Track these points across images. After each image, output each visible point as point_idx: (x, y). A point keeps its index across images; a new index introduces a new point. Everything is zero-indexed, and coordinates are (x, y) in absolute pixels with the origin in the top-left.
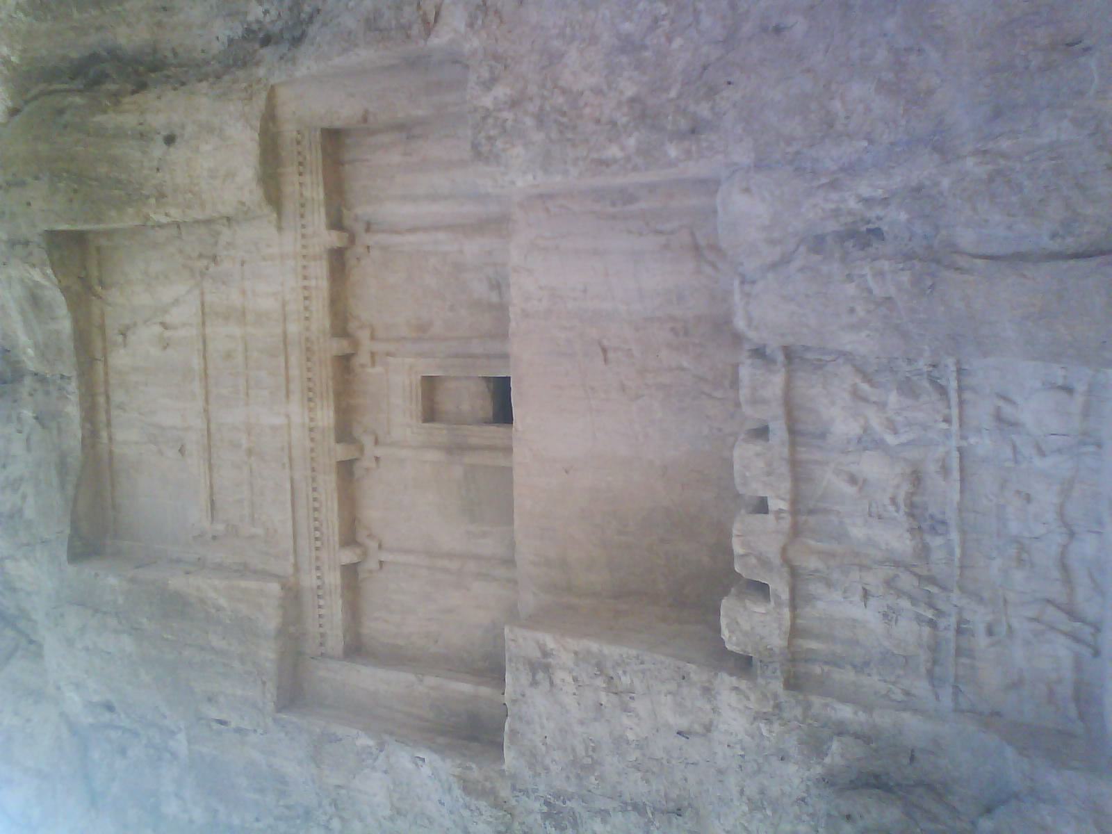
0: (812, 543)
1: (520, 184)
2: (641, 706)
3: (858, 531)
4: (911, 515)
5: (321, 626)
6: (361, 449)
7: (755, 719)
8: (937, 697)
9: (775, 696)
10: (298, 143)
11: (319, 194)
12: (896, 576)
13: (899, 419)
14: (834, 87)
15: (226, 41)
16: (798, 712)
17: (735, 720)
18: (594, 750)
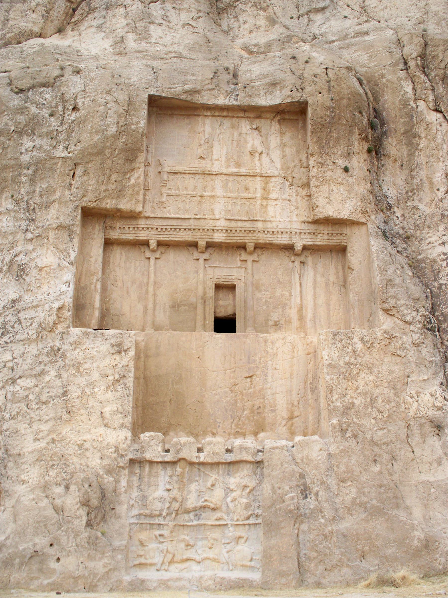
0: (187, 469)
1: (324, 353)
2: (109, 395)
3: (193, 487)
4: (201, 507)
5: (120, 228)
6: (202, 252)
7: (115, 446)
8: (132, 517)
9: (126, 455)
10: (341, 234)
11: (319, 242)
14: (355, 482)
15: (387, 194)
16: (121, 464)
18: (86, 372)
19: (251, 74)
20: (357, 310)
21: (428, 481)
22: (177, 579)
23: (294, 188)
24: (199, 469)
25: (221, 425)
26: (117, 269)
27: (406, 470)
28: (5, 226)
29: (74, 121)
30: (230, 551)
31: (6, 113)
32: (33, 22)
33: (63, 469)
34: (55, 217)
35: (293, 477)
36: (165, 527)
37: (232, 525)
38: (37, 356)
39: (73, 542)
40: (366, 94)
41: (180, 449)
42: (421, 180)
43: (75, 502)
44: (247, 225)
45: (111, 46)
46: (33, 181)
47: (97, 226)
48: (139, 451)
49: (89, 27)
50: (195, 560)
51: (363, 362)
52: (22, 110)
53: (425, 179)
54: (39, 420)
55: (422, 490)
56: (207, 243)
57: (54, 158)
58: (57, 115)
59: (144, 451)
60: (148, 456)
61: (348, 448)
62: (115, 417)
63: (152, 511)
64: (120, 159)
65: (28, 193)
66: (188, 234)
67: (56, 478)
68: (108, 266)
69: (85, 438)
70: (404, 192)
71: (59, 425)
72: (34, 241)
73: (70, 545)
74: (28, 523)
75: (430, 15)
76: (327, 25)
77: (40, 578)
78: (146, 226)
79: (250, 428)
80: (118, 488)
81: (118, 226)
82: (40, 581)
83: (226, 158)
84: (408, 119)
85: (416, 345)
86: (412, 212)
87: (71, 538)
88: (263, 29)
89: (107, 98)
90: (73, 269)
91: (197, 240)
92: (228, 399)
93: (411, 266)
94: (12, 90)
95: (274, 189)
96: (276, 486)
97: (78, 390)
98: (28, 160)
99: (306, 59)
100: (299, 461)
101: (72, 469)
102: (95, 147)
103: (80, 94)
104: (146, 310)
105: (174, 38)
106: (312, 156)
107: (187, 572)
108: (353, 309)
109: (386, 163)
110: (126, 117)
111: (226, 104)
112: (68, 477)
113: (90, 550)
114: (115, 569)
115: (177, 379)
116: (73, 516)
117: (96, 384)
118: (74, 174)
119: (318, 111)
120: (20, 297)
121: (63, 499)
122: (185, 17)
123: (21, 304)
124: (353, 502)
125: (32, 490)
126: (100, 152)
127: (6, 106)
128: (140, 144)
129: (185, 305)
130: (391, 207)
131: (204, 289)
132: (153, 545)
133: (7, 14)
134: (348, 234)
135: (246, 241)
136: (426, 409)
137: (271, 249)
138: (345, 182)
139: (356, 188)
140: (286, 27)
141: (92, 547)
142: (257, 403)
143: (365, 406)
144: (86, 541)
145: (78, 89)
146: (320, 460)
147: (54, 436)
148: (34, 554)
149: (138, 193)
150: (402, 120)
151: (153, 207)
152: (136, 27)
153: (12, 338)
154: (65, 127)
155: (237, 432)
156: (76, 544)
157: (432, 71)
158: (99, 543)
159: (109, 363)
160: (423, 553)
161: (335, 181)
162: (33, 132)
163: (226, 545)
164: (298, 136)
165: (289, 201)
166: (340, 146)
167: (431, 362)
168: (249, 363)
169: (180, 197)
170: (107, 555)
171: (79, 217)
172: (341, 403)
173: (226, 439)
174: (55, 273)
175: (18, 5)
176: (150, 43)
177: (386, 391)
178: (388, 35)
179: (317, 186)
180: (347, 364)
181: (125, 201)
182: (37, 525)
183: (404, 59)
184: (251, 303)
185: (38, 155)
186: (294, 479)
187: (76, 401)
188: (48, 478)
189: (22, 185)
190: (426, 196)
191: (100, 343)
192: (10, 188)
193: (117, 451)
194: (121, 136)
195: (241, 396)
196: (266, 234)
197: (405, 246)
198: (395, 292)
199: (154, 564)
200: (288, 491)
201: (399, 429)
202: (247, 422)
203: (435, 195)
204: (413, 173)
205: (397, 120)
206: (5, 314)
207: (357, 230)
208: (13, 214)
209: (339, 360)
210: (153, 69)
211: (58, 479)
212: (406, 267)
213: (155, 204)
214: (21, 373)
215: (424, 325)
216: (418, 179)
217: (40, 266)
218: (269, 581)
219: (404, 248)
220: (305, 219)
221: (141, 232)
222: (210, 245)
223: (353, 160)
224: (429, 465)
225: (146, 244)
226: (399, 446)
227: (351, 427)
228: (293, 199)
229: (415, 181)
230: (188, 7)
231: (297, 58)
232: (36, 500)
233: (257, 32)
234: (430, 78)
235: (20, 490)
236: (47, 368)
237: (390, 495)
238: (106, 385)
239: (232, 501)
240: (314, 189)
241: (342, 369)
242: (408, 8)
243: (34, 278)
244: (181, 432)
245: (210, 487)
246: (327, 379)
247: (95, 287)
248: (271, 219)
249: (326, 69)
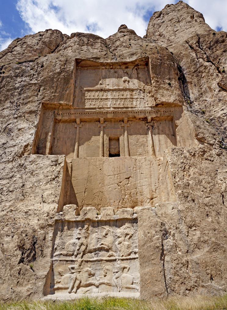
2: (48, 186)
3: (94, 236)
5: (62, 114)
9: (53, 218)
10: (170, 111)
12: (84, 245)
13: (122, 244)
16: (50, 223)
17: (47, 208)
25: (113, 204)
36: (75, 262)
37: (119, 260)
38: (12, 169)
41: (86, 213)
59: (65, 215)
61: (190, 207)
69: (30, 208)
70: (198, 95)
71: (17, 202)
73: (6, 275)
87: (7, 270)
96: (147, 231)
107: (90, 293)
117: (41, 180)
123: (7, 145)
133: (24, 51)
138: (169, 89)
139: (175, 91)
146: (173, 214)
158: (27, 274)
165: (143, 99)
170: (31, 282)
171: (40, 107)
180: (183, 163)
186: (158, 226)
187: (28, 189)
194: (62, 73)
195: (124, 188)
199: (67, 288)
200: (155, 234)
202: (127, 201)
204: (201, 87)
208: (9, 108)
211: (8, 232)
229: (203, 90)
236: (15, 174)
239: (119, 244)
245: (105, 235)
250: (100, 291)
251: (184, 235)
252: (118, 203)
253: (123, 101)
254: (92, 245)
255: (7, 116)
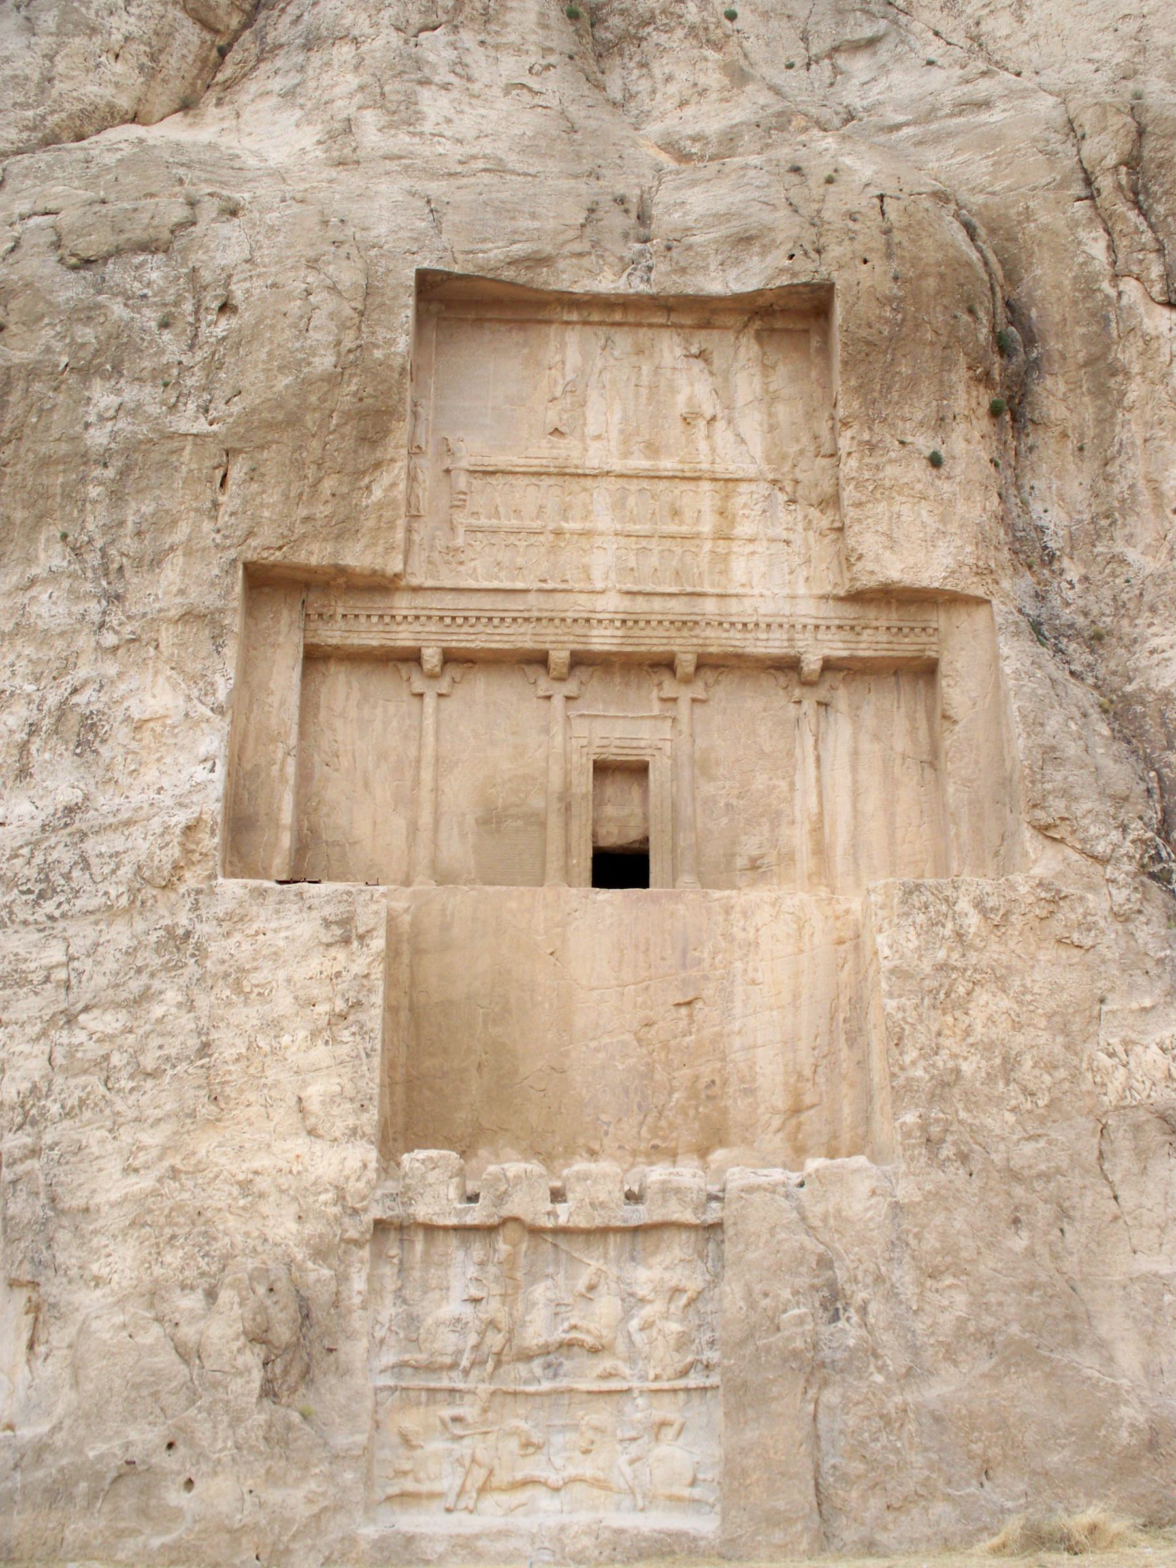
0: (524, 1246)
1: (881, 939)
2: (320, 1053)
3: (540, 1292)
4: (561, 1345)
5: (344, 616)
6: (561, 679)
7: (337, 1187)
8: (382, 1371)
10: (924, 629)
11: (864, 652)
13: (654, 1333)
14: (964, 1278)
16: (352, 1234)
18: (259, 994)
19: (685, 214)
20: (965, 828)
21: (1155, 1275)
22: (499, 1532)
23: (799, 510)
24: (555, 1246)
25: (612, 1130)
26: (338, 723)
27: (1099, 1245)
28: (46, 615)
29: (224, 338)
30: (639, 1459)
31: (46, 320)
32: (117, 84)
33: (201, 1247)
34: (175, 589)
35: (801, 1264)
38: (131, 953)
39: (227, 1438)
40: (986, 264)
41: (505, 1192)
42: (1131, 487)
43: (231, 1332)
44: (677, 607)
45: (319, 142)
46: (117, 497)
47: (285, 613)
48: (399, 1200)
49: (262, 95)
50: (545, 1484)
51: (984, 963)
52: (87, 313)
53: (1141, 484)
54: (137, 1120)
55: (1140, 1299)
56: (573, 654)
57: (171, 436)
58: (180, 325)
59: (410, 1199)
60: (422, 1211)
61: (944, 1187)
62: (335, 1111)
63: (432, 1355)
64: (343, 437)
65: (106, 528)
66: (522, 630)
67: (182, 1270)
68: (316, 716)
69: (256, 1165)
70: (1086, 517)
71: (188, 1132)
72: (120, 652)
73: (220, 1445)
74: (111, 1389)
75: (1152, 55)
76: (883, 83)
77: (140, 1532)
78: (413, 612)
79: (686, 1136)
80: (344, 1295)
81: (341, 611)
82: (141, 1539)
83: (622, 432)
84: (1094, 328)
85: (1120, 917)
86: (1107, 571)
87: (221, 1427)
88: (714, 96)
89: (309, 280)
90: (222, 724)
91: (547, 646)
92: (631, 1061)
93: (1106, 711)
94: (61, 260)
95: (747, 512)
97: (238, 1041)
98: (105, 442)
99: (828, 172)
100: (817, 1223)
101: (224, 1246)
102: (280, 406)
103: (239, 268)
104: (413, 828)
105: (484, 122)
106: (845, 424)
107: (527, 1515)
108: (956, 824)
109: (1040, 443)
110: (359, 328)
111: (621, 291)
112: (214, 1268)
113: (272, 1457)
114: (338, 1508)
115: (497, 1009)
116: (227, 1368)
117: (285, 1023)
118: (225, 476)
119: (861, 306)
120: (86, 798)
121: (202, 1324)
122: (510, 67)
124: (958, 1329)
125: (121, 1303)
126: (293, 421)
127: (47, 302)
128: (396, 397)
129: (516, 817)
130: (1052, 557)
131: (567, 774)
132: (437, 1445)
133: (48, 64)
134: (942, 629)
135: (675, 648)
136: (1148, 1084)
137: (739, 668)
138: (931, 493)
139: (961, 508)
140: (776, 90)
141: (277, 1450)
142: (706, 1071)
143: (990, 1078)
144: (261, 1433)
145: (233, 256)
146: (871, 1219)
147: (177, 1161)
148: (127, 1468)
149: (391, 526)
150: (1081, 330)
151: (430, 562)
152: (383, 94)
153: (65, 907)
154: (200, 355)
155: (655, 1147)
156: (236, 1442)
157: (1158, 201)
158: (296, 1440)
159: (319, 968)
160: (1144, 1463)
161: (906, 491)
162: (117, 370)
163: (626, 1444)
164: (808, 376)
165: (787, 542)
166: (919, 399)
167: (1160, 962)
168: (684, 966)
169: (502, 535)
170: (317, 1470)
171: (238, 589)
172: (926, 1070)
173: (626, 1166)
174: (176, 736)
175: (77, 40)
176: (422, 134)
177: (1044, 1037)
178: (1042, 108)
179: (859, 505)
180: (942, 967)
181: (359, 547)
182: (133, 1394)
183: (1085, 171)
184: (689, 811)
185: (130, 428)
186: (804, 1269)
187: (232, 1068)
188: (162, 1271)
189: (89, 507)
190: (1145, 527)
191: (295, 918)
192: (58, 514)
193: (341, 1198)
194: (346, 377)
195: (663, 1055)
196: (727, 631)
197: (1091, 658)
198: (1066, 778)
200: (789, 1301)
201: (1079, 1137)
202: (679, 1120)
203: (1168, 526)
204: (1110, 469)
205: (1068, 329)
206: (46, 844)
207: (964, 617)
208: (66, 584)
209: (920, 956)
210: (429, 202)
211: (187, 1273)
212: (1095, 714)
213: (436, 555)
214: (89, 996)
215: (1143, 866)
216: (1125, 484)
217: (136, 717)
218: (741, 1536)
219: (1089, 665)
220: (828, 589)
221: (401, 628)
222: (580, 661)
223: (954, 436)
224: (1158, 1231)
225: (413, 657)
226: (1078, 1182)
227: (952, 1133)
228: (797, 538)
229: (1116, 489)
230: (519, 41)
231: (805, 171)
232: (131, 1329)
233: (698, 103)
234: (1153, 220)
235: (87, 1302)
236: (157, 985)
237: (1057, 1310)
238: (312, 1026)
239: (642, 1329)
240: (852, 513)
241: (927, 982)
242: (1094, 38)
243: (122, 750)
244: (508, 1150)
245: (583, 1291)
246: (889, 1009)
247: (281, 770)
248: (741, 591)
249: (881, 198)
250: (566, 1508)
251: (903, 1307)
252: (635, 1130)
253: (679, 550)
254: (530, 1330)
255: (62, 634)
